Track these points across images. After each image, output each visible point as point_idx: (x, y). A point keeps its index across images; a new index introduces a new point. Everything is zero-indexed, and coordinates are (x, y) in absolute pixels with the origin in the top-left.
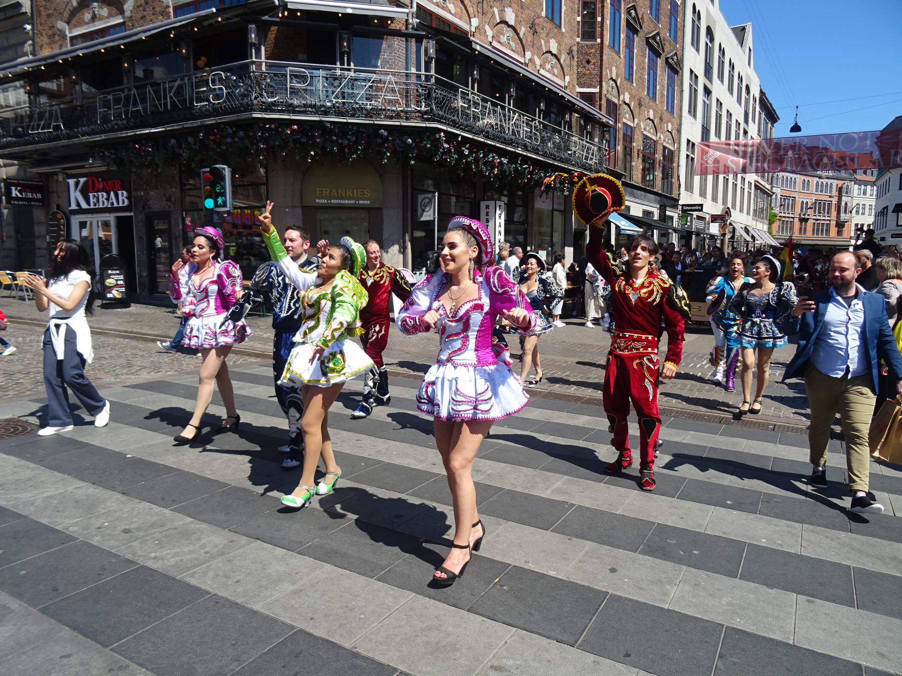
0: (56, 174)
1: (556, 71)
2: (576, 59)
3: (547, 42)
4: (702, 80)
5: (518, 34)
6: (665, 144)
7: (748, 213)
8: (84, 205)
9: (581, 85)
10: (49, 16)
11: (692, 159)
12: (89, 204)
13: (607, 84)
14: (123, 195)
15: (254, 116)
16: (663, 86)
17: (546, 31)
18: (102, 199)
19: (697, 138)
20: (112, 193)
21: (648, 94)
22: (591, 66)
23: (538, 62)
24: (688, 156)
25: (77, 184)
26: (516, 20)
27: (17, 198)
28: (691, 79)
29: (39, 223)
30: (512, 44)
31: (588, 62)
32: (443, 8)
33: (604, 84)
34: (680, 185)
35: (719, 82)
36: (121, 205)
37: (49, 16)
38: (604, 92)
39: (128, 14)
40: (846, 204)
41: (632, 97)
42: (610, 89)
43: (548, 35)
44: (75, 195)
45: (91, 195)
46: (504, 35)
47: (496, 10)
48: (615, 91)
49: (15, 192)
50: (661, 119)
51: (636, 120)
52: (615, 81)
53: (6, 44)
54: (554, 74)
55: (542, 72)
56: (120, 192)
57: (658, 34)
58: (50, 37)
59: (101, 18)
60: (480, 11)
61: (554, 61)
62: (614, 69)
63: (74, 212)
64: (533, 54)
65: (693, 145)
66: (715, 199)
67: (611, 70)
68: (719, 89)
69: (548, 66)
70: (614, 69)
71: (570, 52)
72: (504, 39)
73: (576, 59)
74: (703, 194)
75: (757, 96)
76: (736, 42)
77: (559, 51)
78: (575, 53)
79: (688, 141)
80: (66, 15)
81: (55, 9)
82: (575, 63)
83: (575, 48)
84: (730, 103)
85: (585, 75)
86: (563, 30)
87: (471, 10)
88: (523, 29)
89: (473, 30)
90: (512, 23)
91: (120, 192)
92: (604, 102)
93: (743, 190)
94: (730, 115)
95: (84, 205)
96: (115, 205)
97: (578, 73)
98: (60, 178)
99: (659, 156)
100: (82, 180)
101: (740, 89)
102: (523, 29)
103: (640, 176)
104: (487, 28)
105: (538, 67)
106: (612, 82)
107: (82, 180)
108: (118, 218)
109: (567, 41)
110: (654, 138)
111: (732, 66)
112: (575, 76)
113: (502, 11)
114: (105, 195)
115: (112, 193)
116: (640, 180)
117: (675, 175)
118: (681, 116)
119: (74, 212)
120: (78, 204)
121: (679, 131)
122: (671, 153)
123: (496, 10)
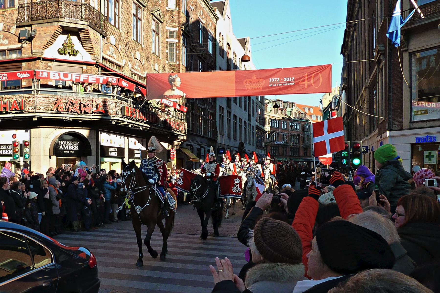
11: (223, 116)
26: (141, 57)
47: (132, 54)
65: (223, 108)
79: (220, 107)
90: (139, 59)
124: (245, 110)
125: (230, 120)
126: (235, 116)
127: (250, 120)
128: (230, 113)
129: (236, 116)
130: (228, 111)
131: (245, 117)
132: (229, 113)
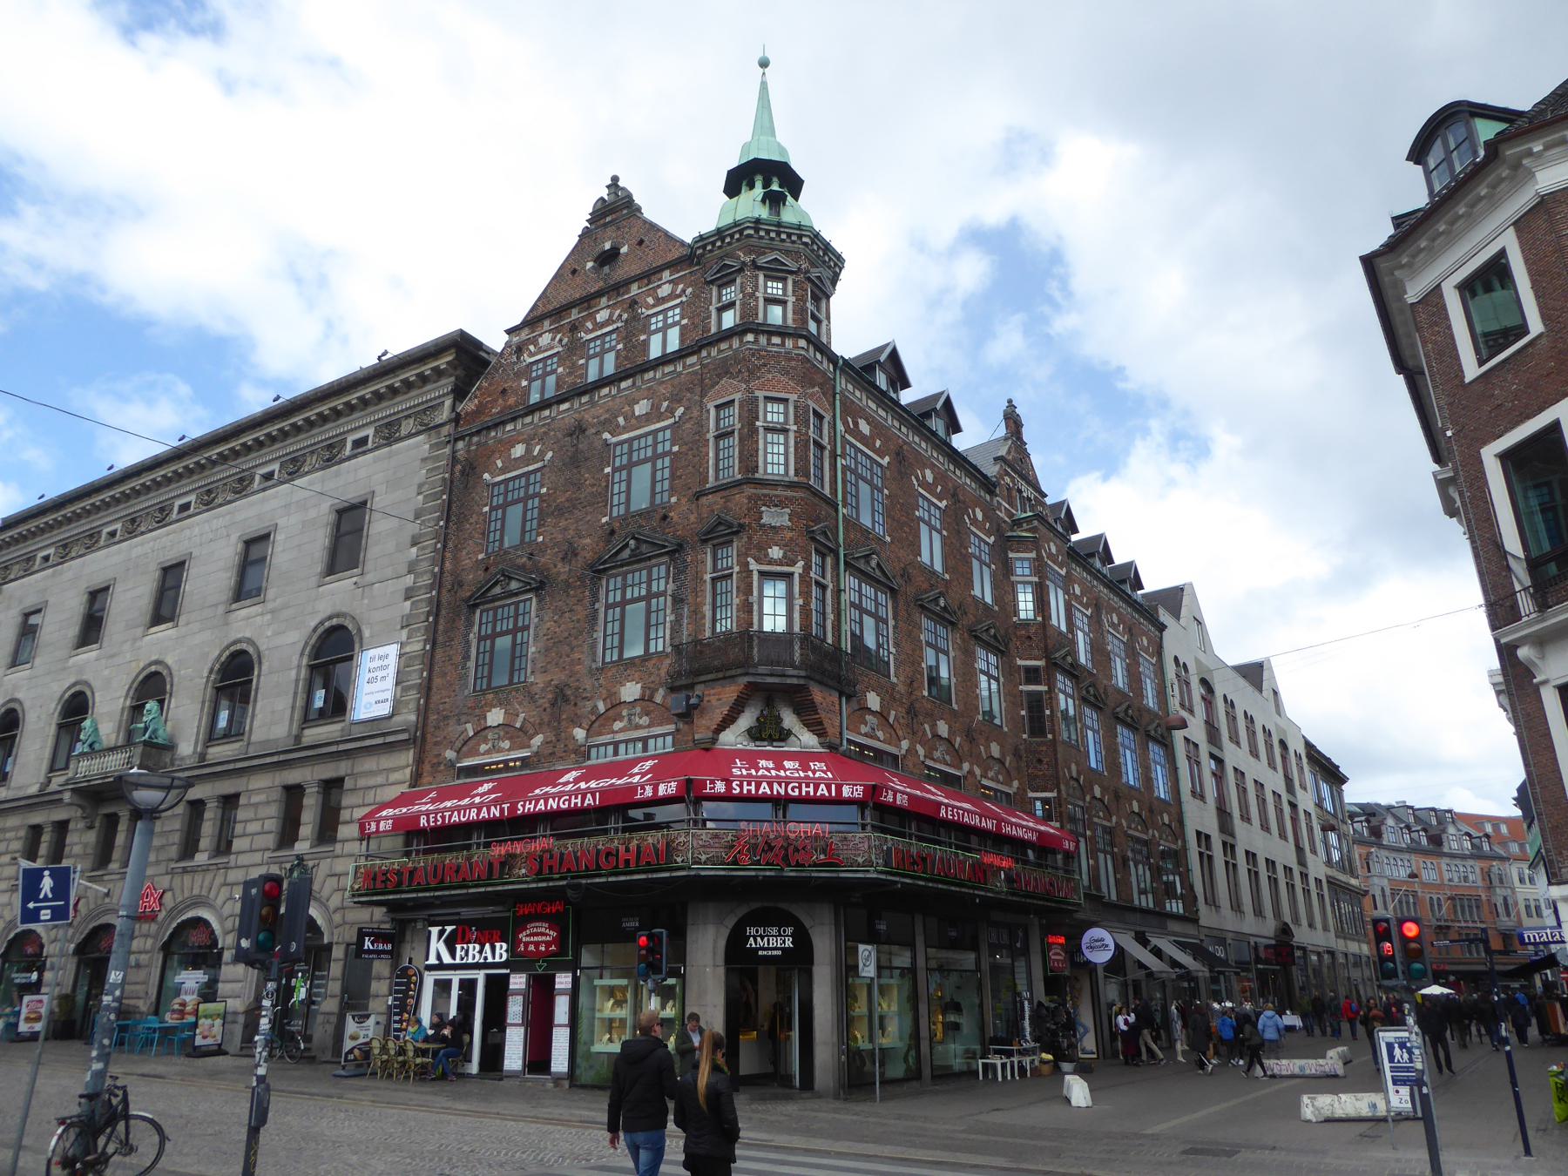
0: (415, 921)
3: (988, 748)
4: (1204, 749)
7: (1326, 929)
8: (447, 959)
10: (436, 744)
12: (454, 957)
13: (1067, 784)
14: (502, 950)
18: (473, 953)
19: (1211, 826)
20: (487, 946)
23: (978, 771)
24: (1201, 854)
25: (441, 933)
27: (369, 952)
29: (379, 979)
31: (1040, 761)
35: (1234, 746)
36: (497, 959)
37: (436, 744)
38: (1064, 795)
39: (535, 749)
40: (1505, 899)
41: (1104, 790)
44: (437, 946)
45: (458, 947)
49: (368, 944)
52: (1077, 780)
53: (375, 768)
55: (985, 782)
56: (498, 945)
59: (500, 750)
62: (1074, 767)
63: (431, 968)
64: (971, 765)
65: (1208, 837)
66: (1258, 912)
67: (1069, 769)
68: (1235, 756)
70: (1074, 767)
74: (1237, 907)
75: (1302, 751)
76: (1250, 689)
77: (1003, 753)
79: (1199, 833)
80: (458, 744)
82: (1023, 765)
84: (1256, 770)
87: (900, 733)
90: (945, 735)
91: (498, 945)
93: (1307, 892)
94: (1259, 786)
95: (447, 959)
96: (490, 960)
98: (420, 925)
100: (449, 929)
101: (1269, 747)
104: (919, 747)
107: (449, 929)
108: (487, 976)
111: (1250, 720)
113: (933, 726)
114: (478, 947)
115: (487, 946)
119: (431, 968)
120: (439, 957)
121: (1181, 822)
124: (1283, 836)
125: (1235, 866)
126: (1251, 856)
127: (1302, 862)
128: (1233, 847)
129: (1254, 855)
130: (1225, 844)
131: (1285, 854)
132: (1229, 848)
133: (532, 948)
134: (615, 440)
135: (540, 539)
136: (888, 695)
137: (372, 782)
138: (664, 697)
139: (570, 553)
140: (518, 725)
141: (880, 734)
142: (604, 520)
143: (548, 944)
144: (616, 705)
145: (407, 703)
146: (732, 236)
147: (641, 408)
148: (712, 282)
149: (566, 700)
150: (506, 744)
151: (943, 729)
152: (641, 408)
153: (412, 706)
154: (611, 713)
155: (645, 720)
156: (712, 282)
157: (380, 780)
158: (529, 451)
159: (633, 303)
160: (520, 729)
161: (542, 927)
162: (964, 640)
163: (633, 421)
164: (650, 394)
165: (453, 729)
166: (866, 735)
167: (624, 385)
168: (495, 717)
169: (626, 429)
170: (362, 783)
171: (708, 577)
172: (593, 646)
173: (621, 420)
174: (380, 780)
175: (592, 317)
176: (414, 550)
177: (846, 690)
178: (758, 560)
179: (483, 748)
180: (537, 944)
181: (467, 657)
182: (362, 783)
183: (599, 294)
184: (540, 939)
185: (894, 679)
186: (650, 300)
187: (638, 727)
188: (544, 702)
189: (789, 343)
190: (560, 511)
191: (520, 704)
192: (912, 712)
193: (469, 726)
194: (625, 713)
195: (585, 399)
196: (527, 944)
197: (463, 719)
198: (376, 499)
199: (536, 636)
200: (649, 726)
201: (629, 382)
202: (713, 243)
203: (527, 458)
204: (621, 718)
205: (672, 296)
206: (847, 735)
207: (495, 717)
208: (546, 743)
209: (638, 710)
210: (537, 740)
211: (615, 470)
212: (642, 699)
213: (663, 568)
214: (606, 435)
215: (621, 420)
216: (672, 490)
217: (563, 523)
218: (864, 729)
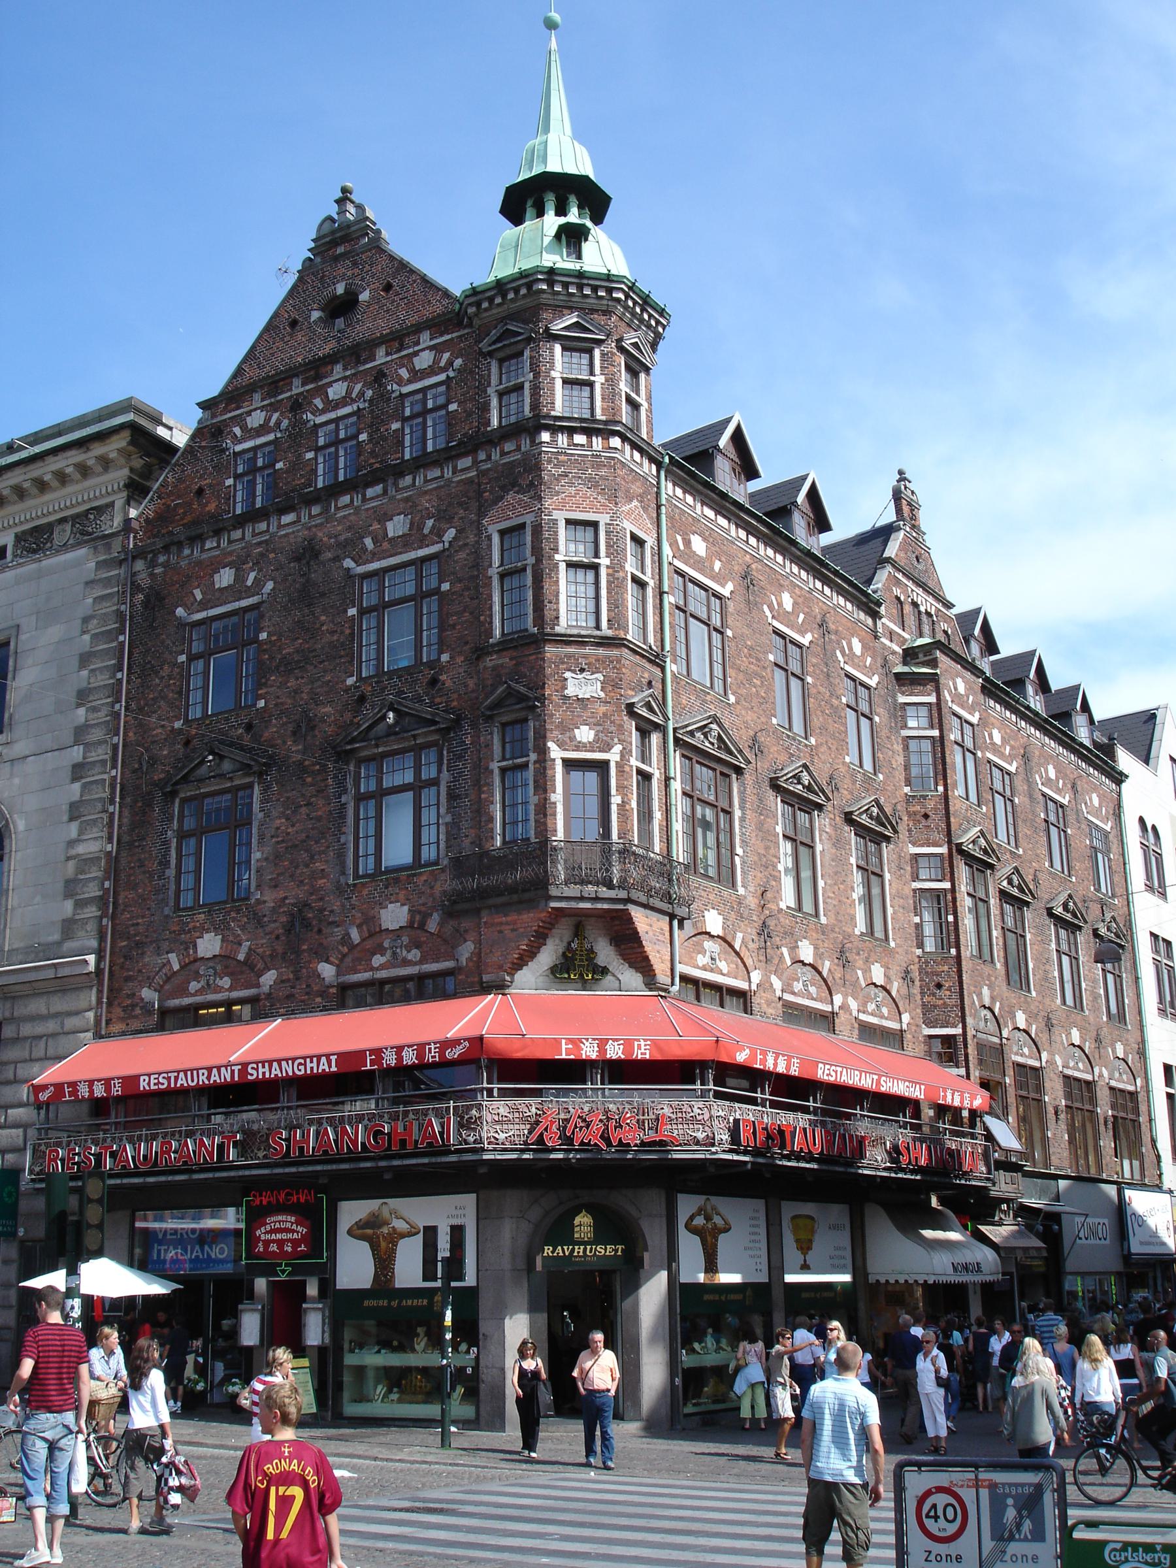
1: (885, 1011)
2: (917, 983)
3: (867, 971)
5: (820, 973)
6: (1113, 1083)
9: (930, 1024)
10: (128, 979)
13: (974, 1016)
15: (485, 1157)
16: (1095, 981)
17: (864, 955)
21: (1064, 1002)
22: (944, 993)
26: (816, 954)
28: (1157, 952)
30: (813, 990)
31: (939, 986)
32: (712, 971)
33: (969, 1020)
34: (1158, 1157)
38: (970, 1032)
39: (266, 989)
41: (1031, 1017)
42: (982, 1024)
43: (867, 960)
46: (798, 980)
47: (785, 950)
48: (992, 1026)
50: (1098, 1040)
51: (1044, 1055)
53: (43, 1011)
54: (882, 1017)
57: (1070, 896)
58: (125, 1009)
59: (219, 989)
60: (763, 958)
61: (882, 994)
62: (986, 991)
64: (845, 996)
67: (980, 995)
69: (871, 1007)
70: (986, 991)
71: (906, 975)
72: (798, 986)
73: (917, 983)
78: (916, 975)
80: (159, 980)
81: (140, 971)
82: (916, 990)
83: (915, 968)
85: (935, 1006)
86: (892, 944)
87: (749, 962)
88: (827, 964)
89: (754, 987)
90: (809, 959)
92: (972, 1050)
97: (923, 1005)
99: (1104, 1109)
102: (827, 964)
103: (1066, 1154)
104: (774, 979)
105: (855, 1013)
106: (986, 1012)
109: (901, 960)
110: (1089, 1077)
112: (919, 1011)
113: (794, 948)
116: (1066, 1163)
117: (1146, 1139)
118: (1141, 1027)
121: (1142, 1053)
122: (1133, 1095)
123: (785, 950)
133: (274, 1248)
134: (361, 570)
135: (261, 703)
136: (735, 911)
137: (40, 1029)
138: (441, 924)
139: (304, 726)
140: (241, 957)
141: (723, 965)
142: (350, 681)
143: (295, 1243)
144: (373, 931)
145: (85, 921)
146: (516, 290)
147: (396, 527)
148: (490, 354)
149: (307, 925)
150: (226, 982)
151: (806, 952)
152: (396, 527)
153: (92, 927)
154: (369, 944)
155: (414, 955)
156: (490, 354)
157: (51, 1026)
158: (240, 578)
159: (379, 376)
160: (245, 963)
161: (287, 1220)
162: (835, 827)
163: (386, 545)
164: (410, 507)
165: (150, 959)
166: (704, 968)
167: (370, 492)
168: (209, 945)
169: (375, 556)
170: (27, 1030)
171: (495, 766)
172: (341, 856)
173: (368, 542)
174: (51, 1026)
175: (322, 391)
176: (81, 711)
177: (681, 911)
178: (561, 745)
179: (194, 986)
180: (281, 1243)
181: (165, 864)
182: (27, 1030)
183: (331, 359)
184: (284, 1236)
185: (741, 891)
186: (404, 373)
187: (406, 963)
188: (277, 927)
189: (597, 443)
190: (287, 667)
191: (243, 928)
192: (764, 931)
193: (173, 957)
194: (386, 944)
195: (316, 510)
196: (267, 1243)
197: (165, 946)
198: (23, 637)
199: (261, 837)
200: (421, 962)
201: (379, 489)
202: (491, 300)
203: (238, 590)
204: (380, 950)
205: (432, 371)
206: (680, 968)
207: (209, 945)
208: (280, 982)
209: (405, 940)
210: (269, 978)
211: (362, 612)
212: (410, 925)
213: (433, 754)
214: (348, 563)
215: (368, 542)
216: (442, 646)
217: (292, 683)
218: (702, 960)
